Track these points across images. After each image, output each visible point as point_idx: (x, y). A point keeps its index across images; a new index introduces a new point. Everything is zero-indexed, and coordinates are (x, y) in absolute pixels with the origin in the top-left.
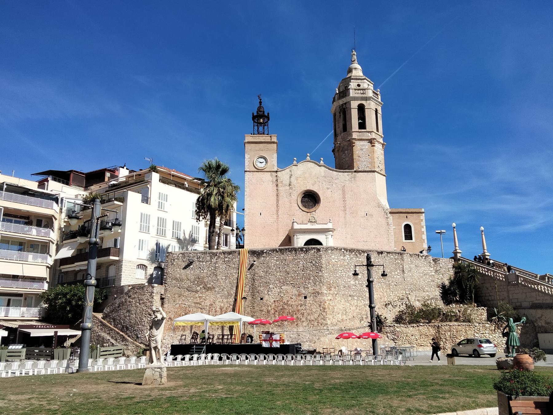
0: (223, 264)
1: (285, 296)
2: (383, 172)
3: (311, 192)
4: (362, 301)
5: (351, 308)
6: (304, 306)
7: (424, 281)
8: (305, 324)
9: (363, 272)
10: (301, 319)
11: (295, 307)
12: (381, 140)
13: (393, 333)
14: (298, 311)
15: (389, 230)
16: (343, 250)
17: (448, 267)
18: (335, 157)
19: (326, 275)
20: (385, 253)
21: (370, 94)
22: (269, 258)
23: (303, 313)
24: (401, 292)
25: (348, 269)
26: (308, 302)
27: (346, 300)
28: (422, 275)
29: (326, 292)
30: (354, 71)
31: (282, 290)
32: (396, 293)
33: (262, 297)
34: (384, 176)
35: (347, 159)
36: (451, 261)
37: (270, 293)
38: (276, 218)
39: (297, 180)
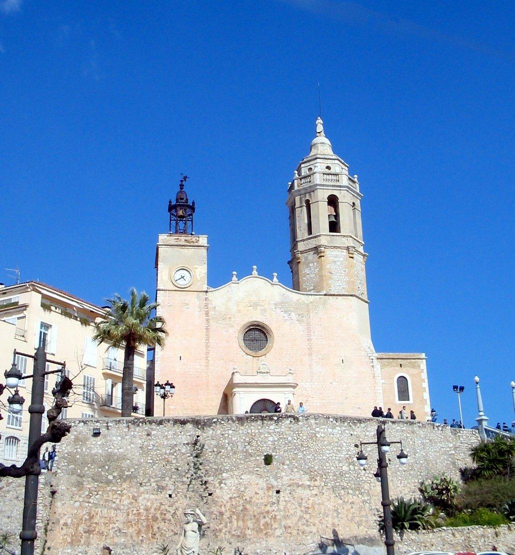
0: (150, 440)
1: (247, 490)
2: (365, 297)
4: (360, 496)
5: (344, 506)
6: (275, 505)
7: (442, 463)
8: (278, 532)
9: (372, 452)
10: (272, 525)
11: (263, 507)
12: (361, 249)
13: (406, 543)
14: (268, 512)
16: (331, 420)
17: (471, 441)
18: (292, 272)
19: (308, 457)
20: (390, 424)
21: (345, 181)
22: (221, 431)
23: (275, 516)
24: (413, 481)
25: (339, 448)
26: (282, 499)
27: (337, 494)
28: (438, 454)
29: (308, 483)
30: (320, 147)
31: (241, 481)
32: (406, 482)
33: (210, 492)
34: (366, 302)
35: (312, 276)
36: (474, 433)
37: (222, 485)
38: (204, 364)
39: (238, 305)
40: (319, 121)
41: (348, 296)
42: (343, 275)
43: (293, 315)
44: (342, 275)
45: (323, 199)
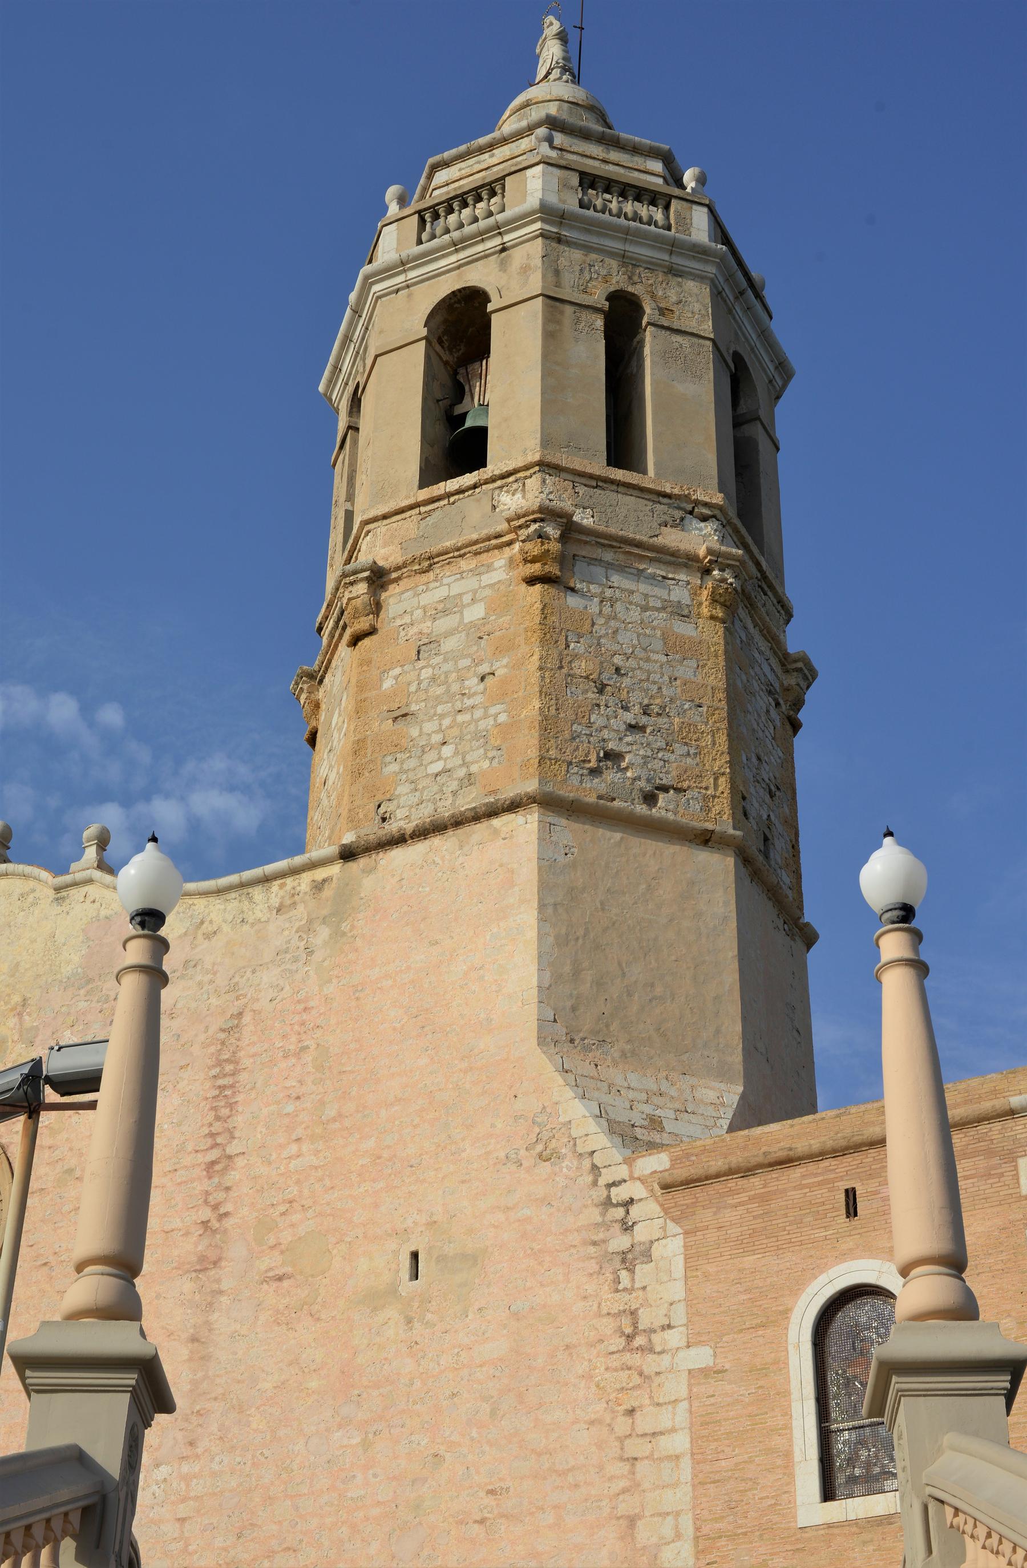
15: (639, 1398)
34: (705, 839)
40: (552, 26)
41: (492, 812)
42: (478, 699)
44: (469, 702)
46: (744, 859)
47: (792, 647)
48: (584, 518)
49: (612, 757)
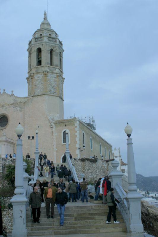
3: (4, 115)
34: (57, 96)
41: (43, 95)
43: (18, 109)
45: (35, 51)
46: (60, 97)
47: (63, 77)
48: (49, 70)
49: (51, 90)
